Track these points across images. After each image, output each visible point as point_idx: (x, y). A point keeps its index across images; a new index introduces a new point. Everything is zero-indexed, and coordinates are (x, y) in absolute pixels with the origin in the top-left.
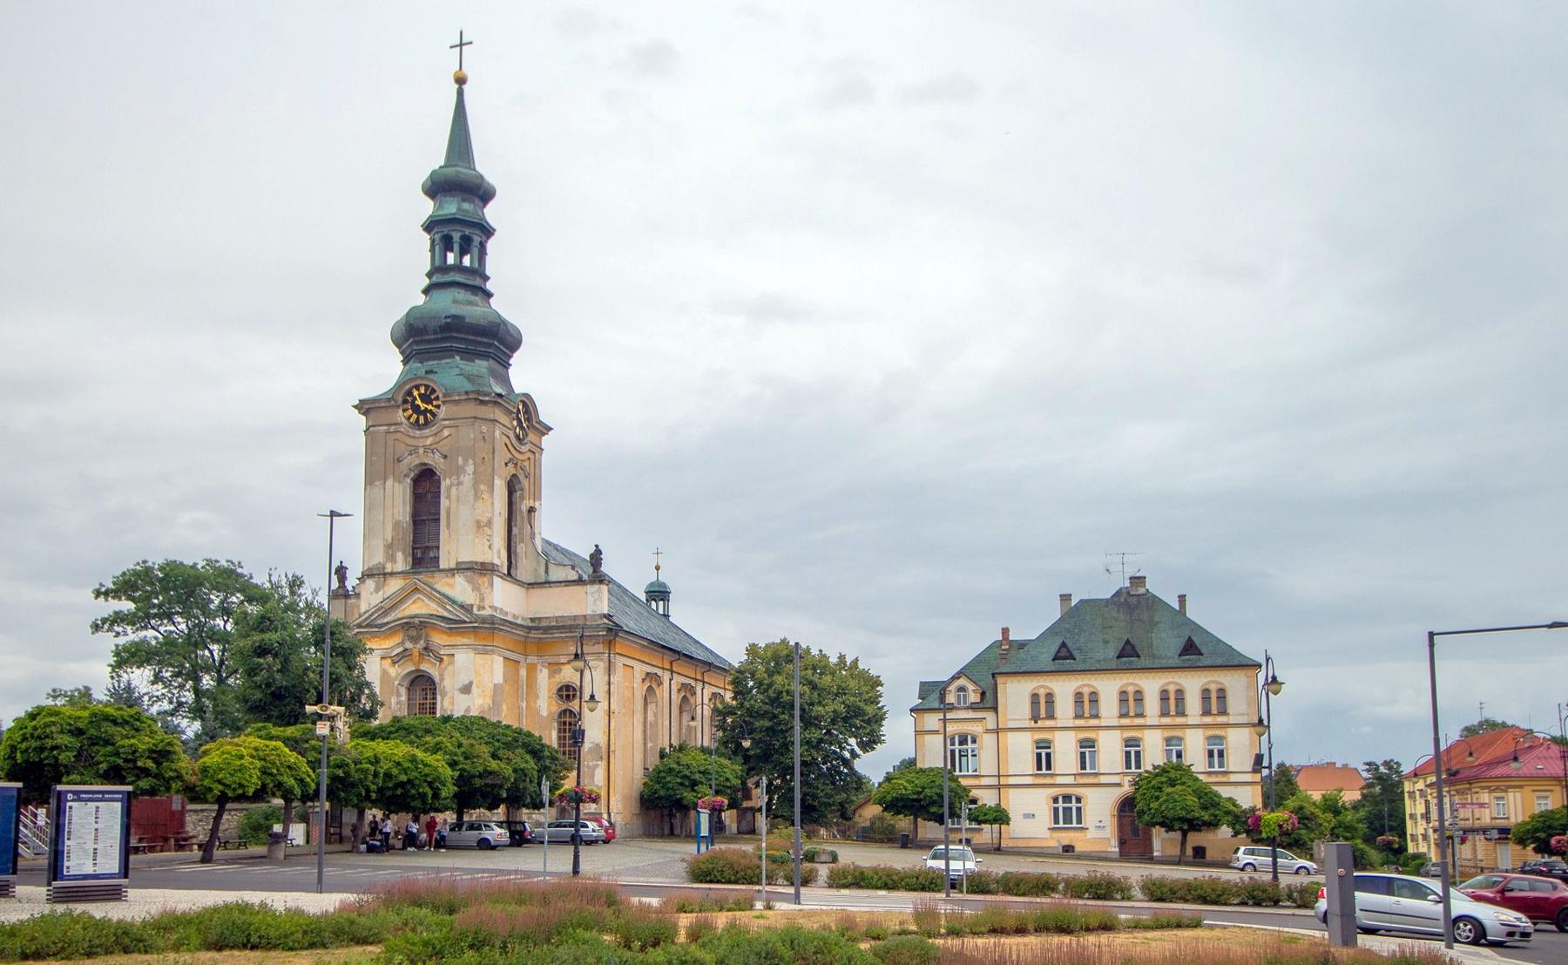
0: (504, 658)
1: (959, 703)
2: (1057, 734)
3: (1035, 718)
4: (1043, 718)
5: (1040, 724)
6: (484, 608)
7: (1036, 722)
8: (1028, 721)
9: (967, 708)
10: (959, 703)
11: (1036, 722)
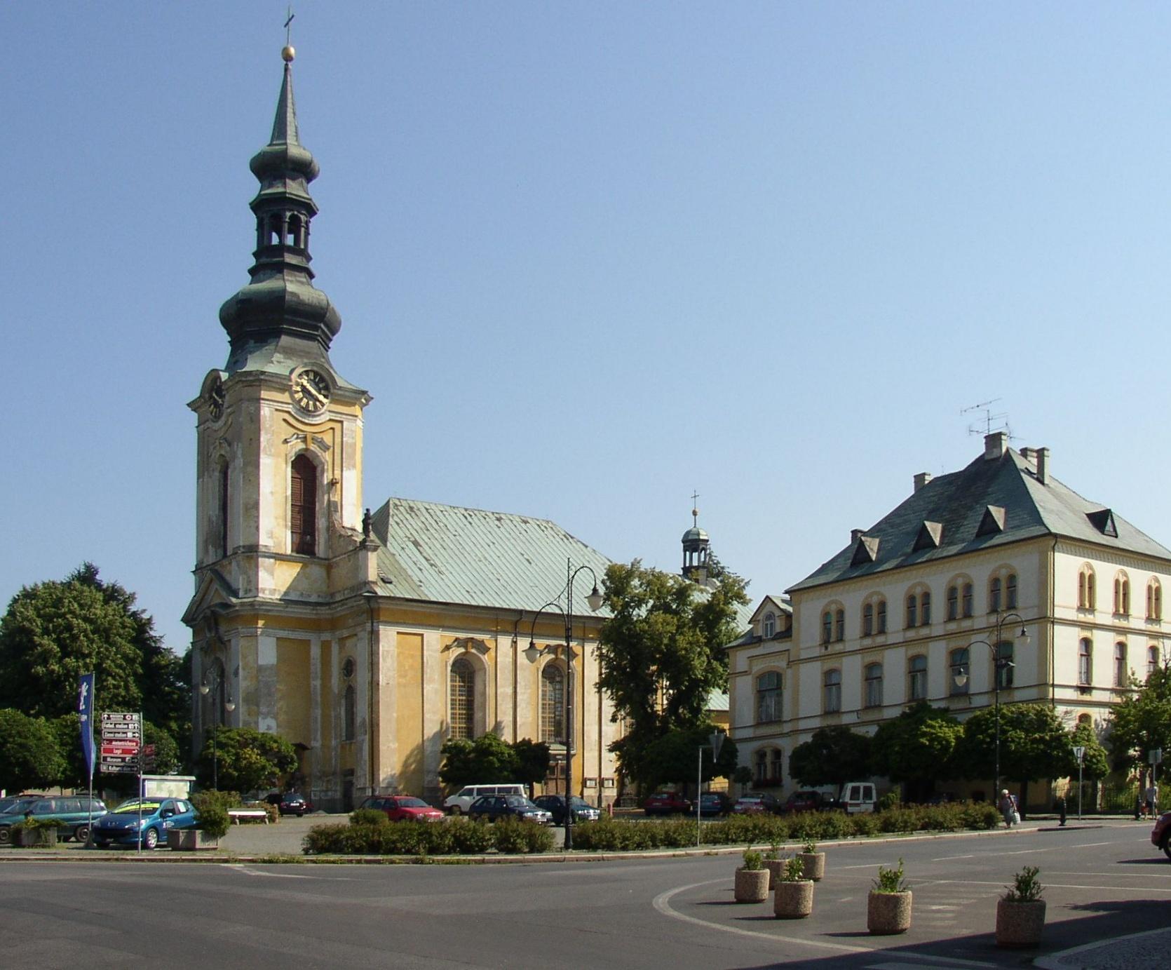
0: (277, 638)
1: (767, 635)
2: (845, 660)
3: (826, 642)
4: (833, 642)
5: (831, 649)
6: (250, 590)
7: (826, 648)
8: (818, 649)
9: (773, 639)
10: (767, 635)
11: (826, 648)
